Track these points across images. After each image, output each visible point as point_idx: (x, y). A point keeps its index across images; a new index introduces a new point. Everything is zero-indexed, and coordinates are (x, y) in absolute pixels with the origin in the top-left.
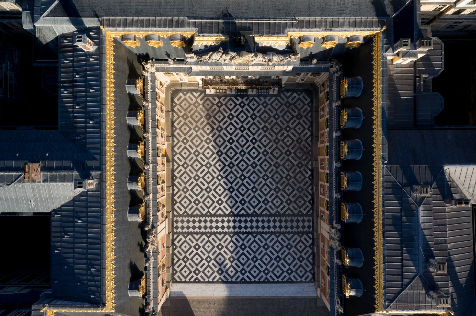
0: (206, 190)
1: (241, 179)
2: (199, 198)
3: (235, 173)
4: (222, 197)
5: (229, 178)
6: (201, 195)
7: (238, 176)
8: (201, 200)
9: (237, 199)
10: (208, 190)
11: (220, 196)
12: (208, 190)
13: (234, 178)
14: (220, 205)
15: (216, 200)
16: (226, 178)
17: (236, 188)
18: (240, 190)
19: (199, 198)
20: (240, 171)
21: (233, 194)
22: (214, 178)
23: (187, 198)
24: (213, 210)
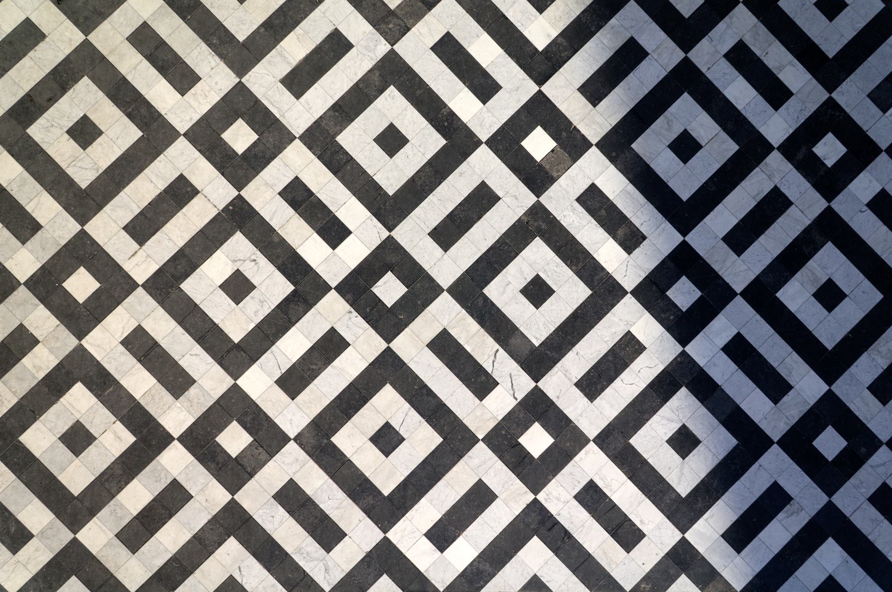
0: (357, 288)
1: (809, 167)
2: (258, 382)
3: (740, 92)
4: (560, 384)
5: (653, 146)
6: (294, 345)
7: (776, 127)
8: (293, 415)
9: (754, 403)
10: (386, 288)
11: (538, 360)
12: (386, 288)
13: (718, 148)
14: (534, 472)
15: (481, 414)
16: (618, 145)
17: (739, 270)
18: (795, 295)
19: (258, 382)
20: (793, 74)
21: (706, 349)
22: (458, 141)
23: (103, 384)
24: (442, 535)
